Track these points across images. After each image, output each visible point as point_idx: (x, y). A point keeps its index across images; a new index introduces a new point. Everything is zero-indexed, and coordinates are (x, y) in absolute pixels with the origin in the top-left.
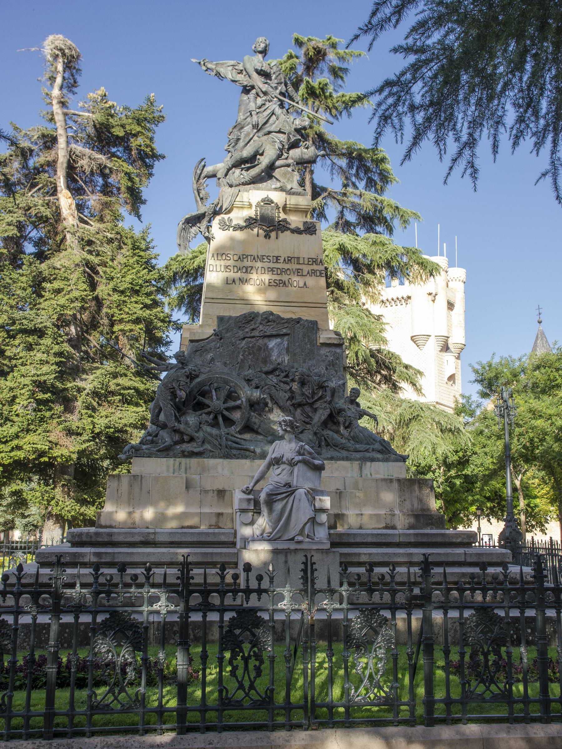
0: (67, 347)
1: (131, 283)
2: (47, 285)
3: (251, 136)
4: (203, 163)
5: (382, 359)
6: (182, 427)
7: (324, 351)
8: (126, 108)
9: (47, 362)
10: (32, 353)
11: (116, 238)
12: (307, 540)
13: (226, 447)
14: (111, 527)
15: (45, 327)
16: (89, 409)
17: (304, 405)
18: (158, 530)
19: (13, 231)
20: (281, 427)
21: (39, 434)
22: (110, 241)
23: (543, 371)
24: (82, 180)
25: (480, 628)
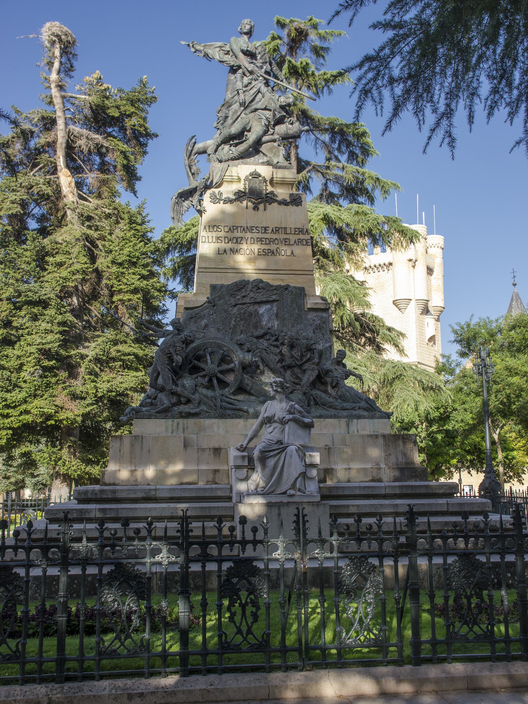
0: (70, 317)
1: (129, 256)
2: (50, 259)
3: (239, 114)
4: (194, 141)
5: (366, 323)
6: (179, 389)
7: (311, 315)
8: (120, 90)
9: (52, 332)
10: (37, 323)
11: (114, 214)
12: (299, 493)
13: (221, 408)
14: (114, 484)
15: (49, 298)
16: (92, 375)
17: (294, 367)
18: (158, 487)
19: (17, 209)
20: (272, 388)
21: (46, 399)
22: (108, 216)
23: (518, 330)
24: (80, 159)
25: (463, 573)
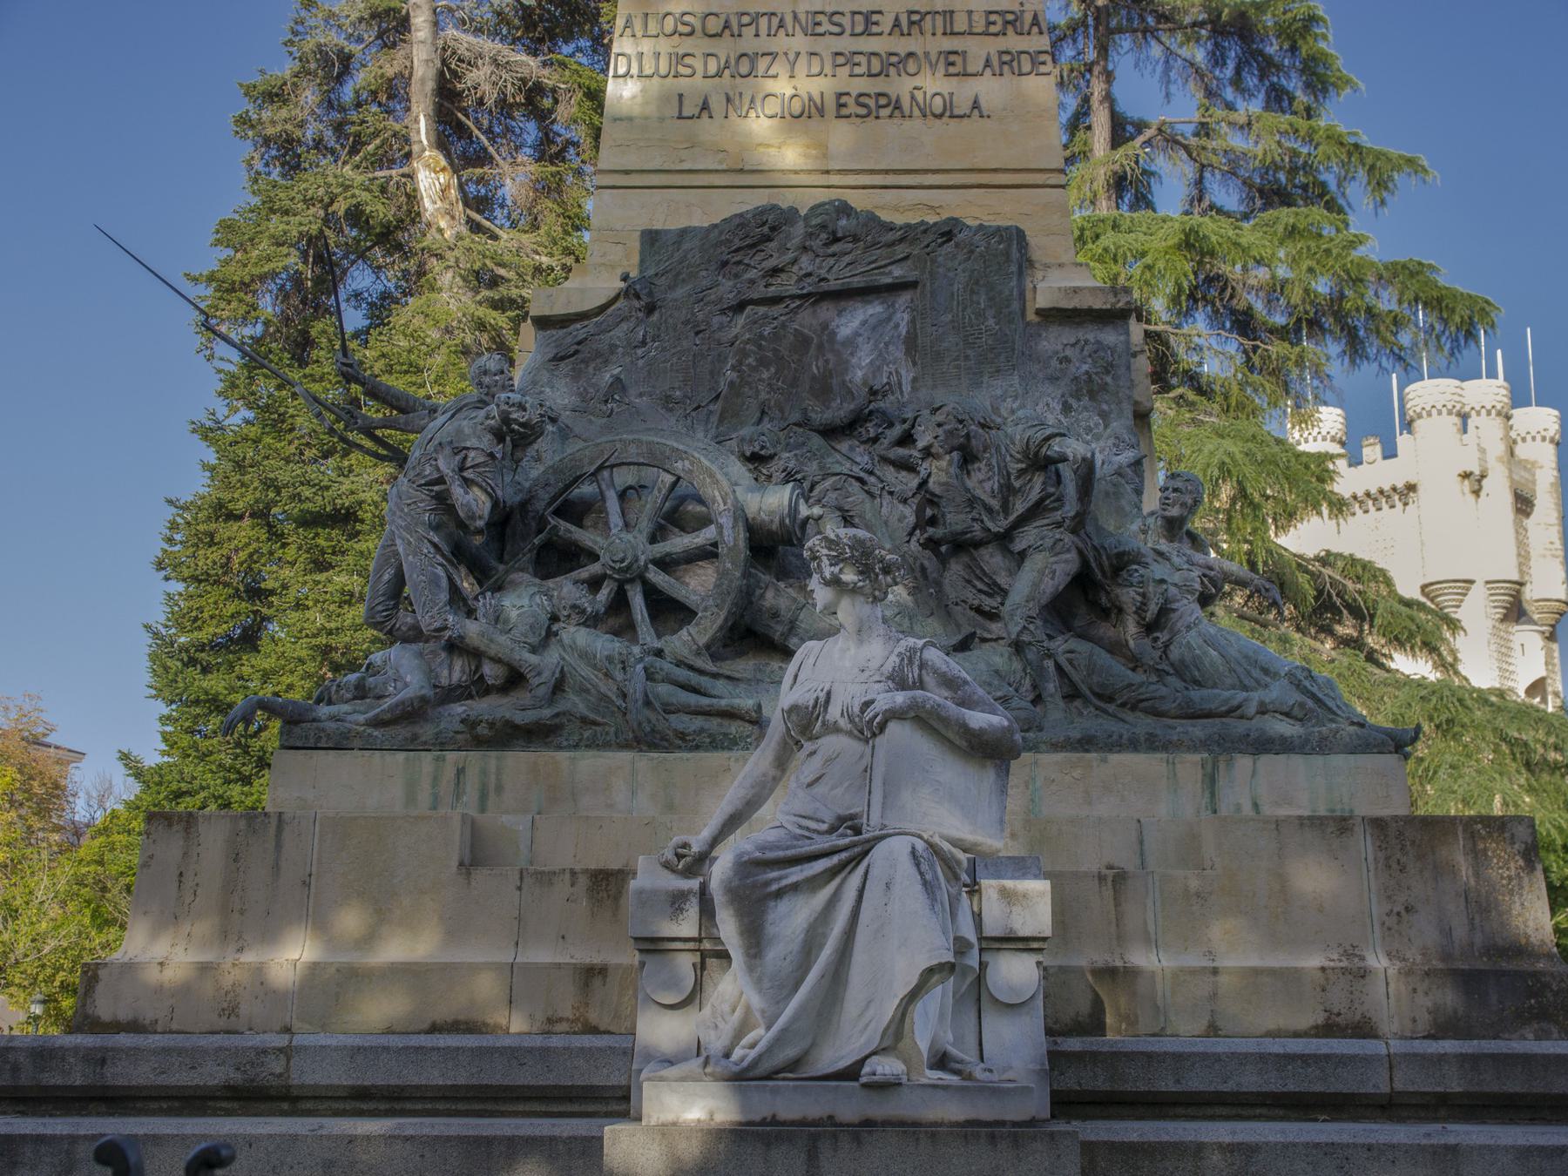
6: (473, 630)
7: (1055, 340)
14: (134, 1027)
15: (360, 503)
17: (977, 544)
24: (477, 122)
